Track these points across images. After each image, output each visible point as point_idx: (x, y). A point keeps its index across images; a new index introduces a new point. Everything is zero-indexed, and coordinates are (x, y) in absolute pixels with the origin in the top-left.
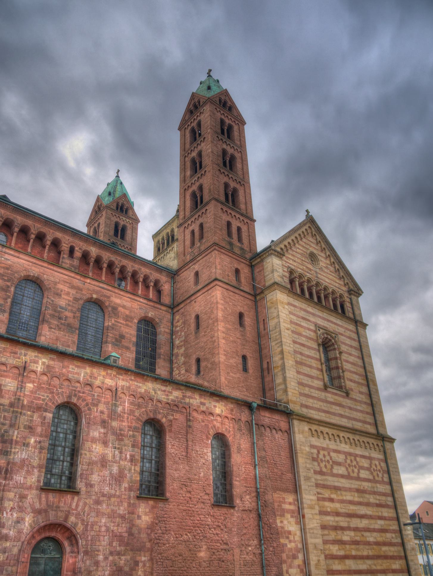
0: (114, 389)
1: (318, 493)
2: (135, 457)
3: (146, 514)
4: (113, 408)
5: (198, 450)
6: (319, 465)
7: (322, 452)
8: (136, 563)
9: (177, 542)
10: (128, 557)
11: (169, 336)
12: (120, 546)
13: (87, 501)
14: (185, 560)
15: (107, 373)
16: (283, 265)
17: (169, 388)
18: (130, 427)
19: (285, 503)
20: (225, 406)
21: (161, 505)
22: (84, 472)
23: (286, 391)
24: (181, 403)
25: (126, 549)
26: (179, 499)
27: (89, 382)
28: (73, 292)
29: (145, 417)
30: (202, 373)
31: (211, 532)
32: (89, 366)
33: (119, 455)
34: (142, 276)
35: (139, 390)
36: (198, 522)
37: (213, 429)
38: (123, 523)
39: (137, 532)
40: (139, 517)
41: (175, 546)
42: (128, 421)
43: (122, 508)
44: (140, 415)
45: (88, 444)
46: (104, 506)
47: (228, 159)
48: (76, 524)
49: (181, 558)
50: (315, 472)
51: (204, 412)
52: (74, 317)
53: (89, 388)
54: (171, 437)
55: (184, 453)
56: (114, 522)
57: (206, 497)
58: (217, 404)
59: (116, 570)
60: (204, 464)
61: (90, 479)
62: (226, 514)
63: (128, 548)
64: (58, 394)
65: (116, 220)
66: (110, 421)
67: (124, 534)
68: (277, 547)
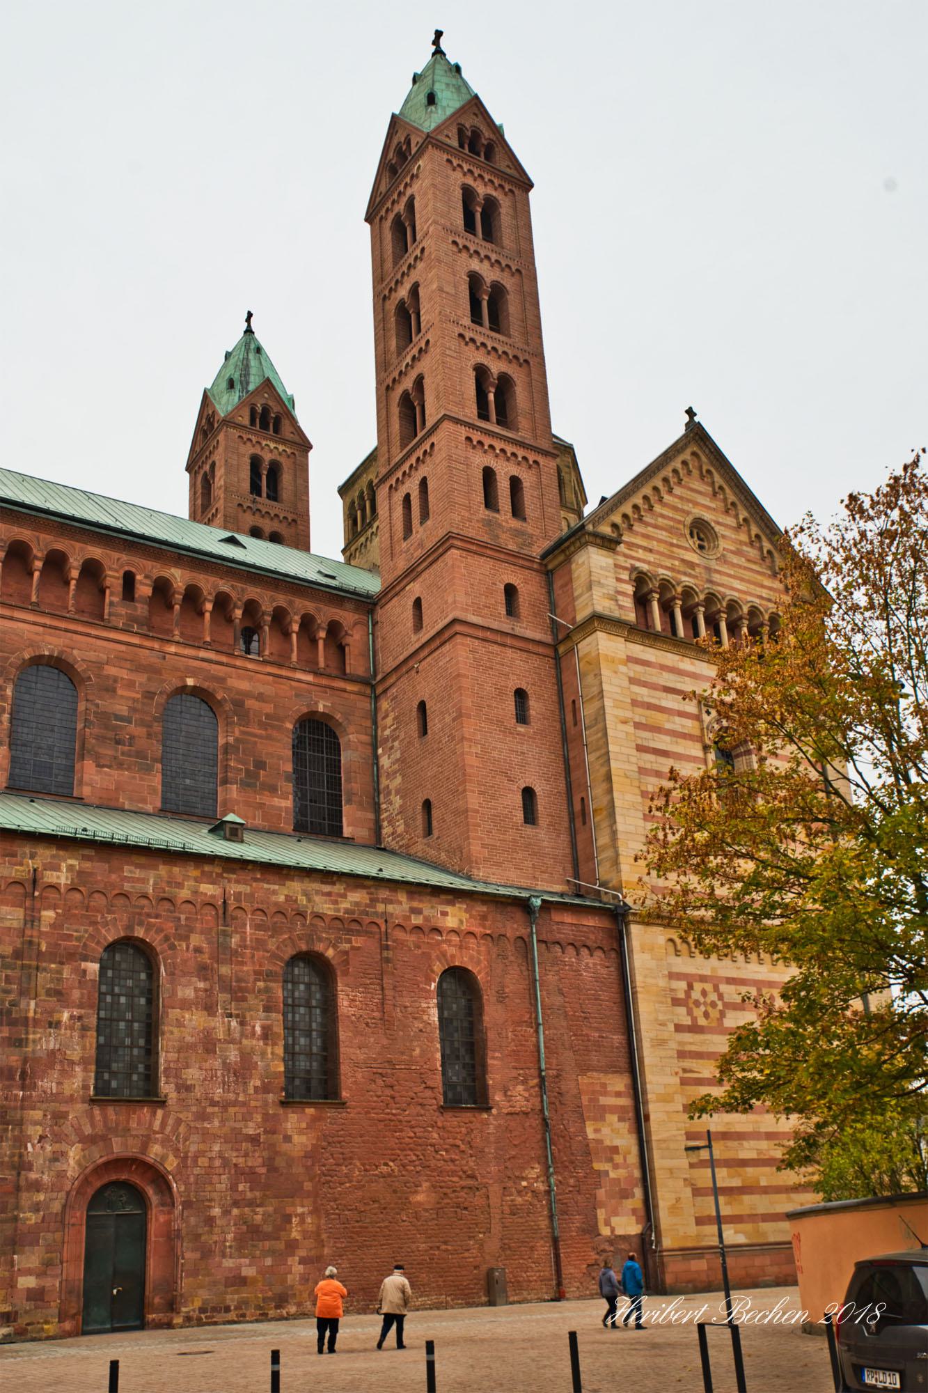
0: (220, 902)
1: (685, 1071)
2: (271, 1030)
3: (301, 1132)
4: (221, 940)
5: (408, 1004)
6: (690, 1013)
7: (698, 986)
8: (287, 1219)
9: (367, 1178)
10: (270, 1209)
11: (369, 751)
12: (251, 1190)
13: (181, 1116)
14: (385, 1208)
15: (203, 872)
16: (616, 566)
17: (339, 888)
18: (256, 973)
19: (605, 1094)
20: (466, 911)
21: (330, 1113)
22: (172, 1065)
23: (616, 862)
24: (367, 914)
25: (265, 1195)
26: (369, 1101)
27: (166, 895)
28: (141, 678)
29: (289, 952)
30: (436, 833)
31: (438, 1157)
32: (164, 863)
33: (239, 1028)
34: (297, 618)
35: (273, 898)
36: (410, 1141)
37: (440, 961)
38: (255, 1151)
39: (283, 1164)
40: (288, 1139)
41: (364, 1186)
42: (253, 963)
43: (251, 1124)
44: (278, 948)
45: (174, 1013)
46: (216, 1123)
47: (486, 298)
48: (164, 1158)
49: (376, 1205)
50: (679, 1028)
51: (418, 928)
52: (149, 736)
53: (167, 905)
54: (347, 985)
55: (376, 1014)
56: (237, 1150)
57: (428, 1093)
58: (449, 909)
59: (248, 1231)
60: (421, 1031)
61: (184, 1077)
62: (471, 1122)
63: (268, 1193)
64: (106, 924)
65: (252, 451)
66: (215, 965)
67: (258, 1170)
68: (585, 1177)
